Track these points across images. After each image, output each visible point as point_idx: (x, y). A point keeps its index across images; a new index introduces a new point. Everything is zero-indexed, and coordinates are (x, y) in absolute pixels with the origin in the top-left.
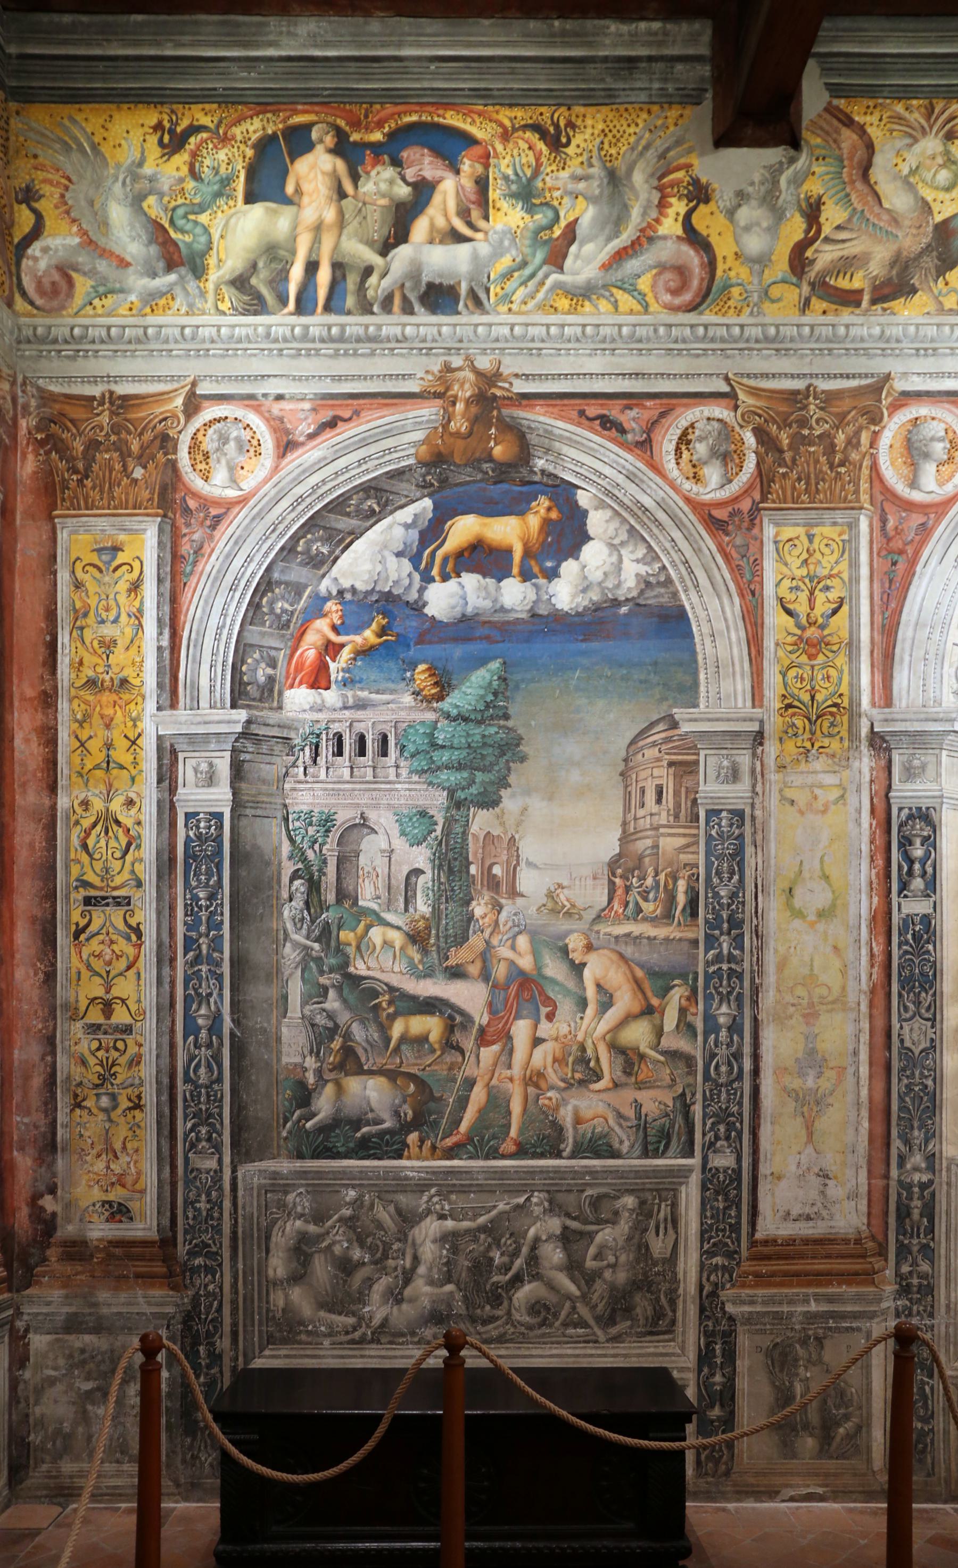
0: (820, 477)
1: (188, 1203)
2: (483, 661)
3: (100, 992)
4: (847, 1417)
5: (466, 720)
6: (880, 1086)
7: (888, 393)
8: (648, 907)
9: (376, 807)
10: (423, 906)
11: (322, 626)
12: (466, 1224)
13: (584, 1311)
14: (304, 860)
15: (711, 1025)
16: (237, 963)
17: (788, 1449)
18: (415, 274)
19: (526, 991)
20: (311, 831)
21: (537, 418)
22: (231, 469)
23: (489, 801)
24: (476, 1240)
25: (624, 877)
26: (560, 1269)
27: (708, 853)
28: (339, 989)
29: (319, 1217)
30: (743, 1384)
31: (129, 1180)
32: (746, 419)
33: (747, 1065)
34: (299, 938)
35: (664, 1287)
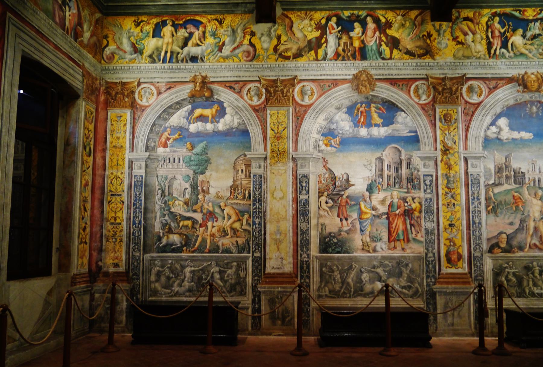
0: (280, 99)
1: (132, 263)
2: (202, 141)
3: (113, 215)
4: (288, 316)
5: (198, 155)
6: (295, 238)
8: (239, 197)
9: (178, 174)
10: (187, 196)
11: (166, 134)
12: (197, 268)
13: (224, 289)
14: (161, 186)
15: (254, 223)
16: (146, 209)
17: (274, 323)
18: (189, 54)
19: (211, 215)
20: (163, 179)
21: (215, 87)
22: (147, 99)
23: (203, 173)
24: (199, 272)
25: (234, 190)
26: (219, 279)
27: (253, 185)
28: (168, 214)
29: (162, 267)
30: (263, 308)
31: (119, 258)
32: (263, 86)
33: (263, 233)
34: (159, 203)
35: (243, 284)
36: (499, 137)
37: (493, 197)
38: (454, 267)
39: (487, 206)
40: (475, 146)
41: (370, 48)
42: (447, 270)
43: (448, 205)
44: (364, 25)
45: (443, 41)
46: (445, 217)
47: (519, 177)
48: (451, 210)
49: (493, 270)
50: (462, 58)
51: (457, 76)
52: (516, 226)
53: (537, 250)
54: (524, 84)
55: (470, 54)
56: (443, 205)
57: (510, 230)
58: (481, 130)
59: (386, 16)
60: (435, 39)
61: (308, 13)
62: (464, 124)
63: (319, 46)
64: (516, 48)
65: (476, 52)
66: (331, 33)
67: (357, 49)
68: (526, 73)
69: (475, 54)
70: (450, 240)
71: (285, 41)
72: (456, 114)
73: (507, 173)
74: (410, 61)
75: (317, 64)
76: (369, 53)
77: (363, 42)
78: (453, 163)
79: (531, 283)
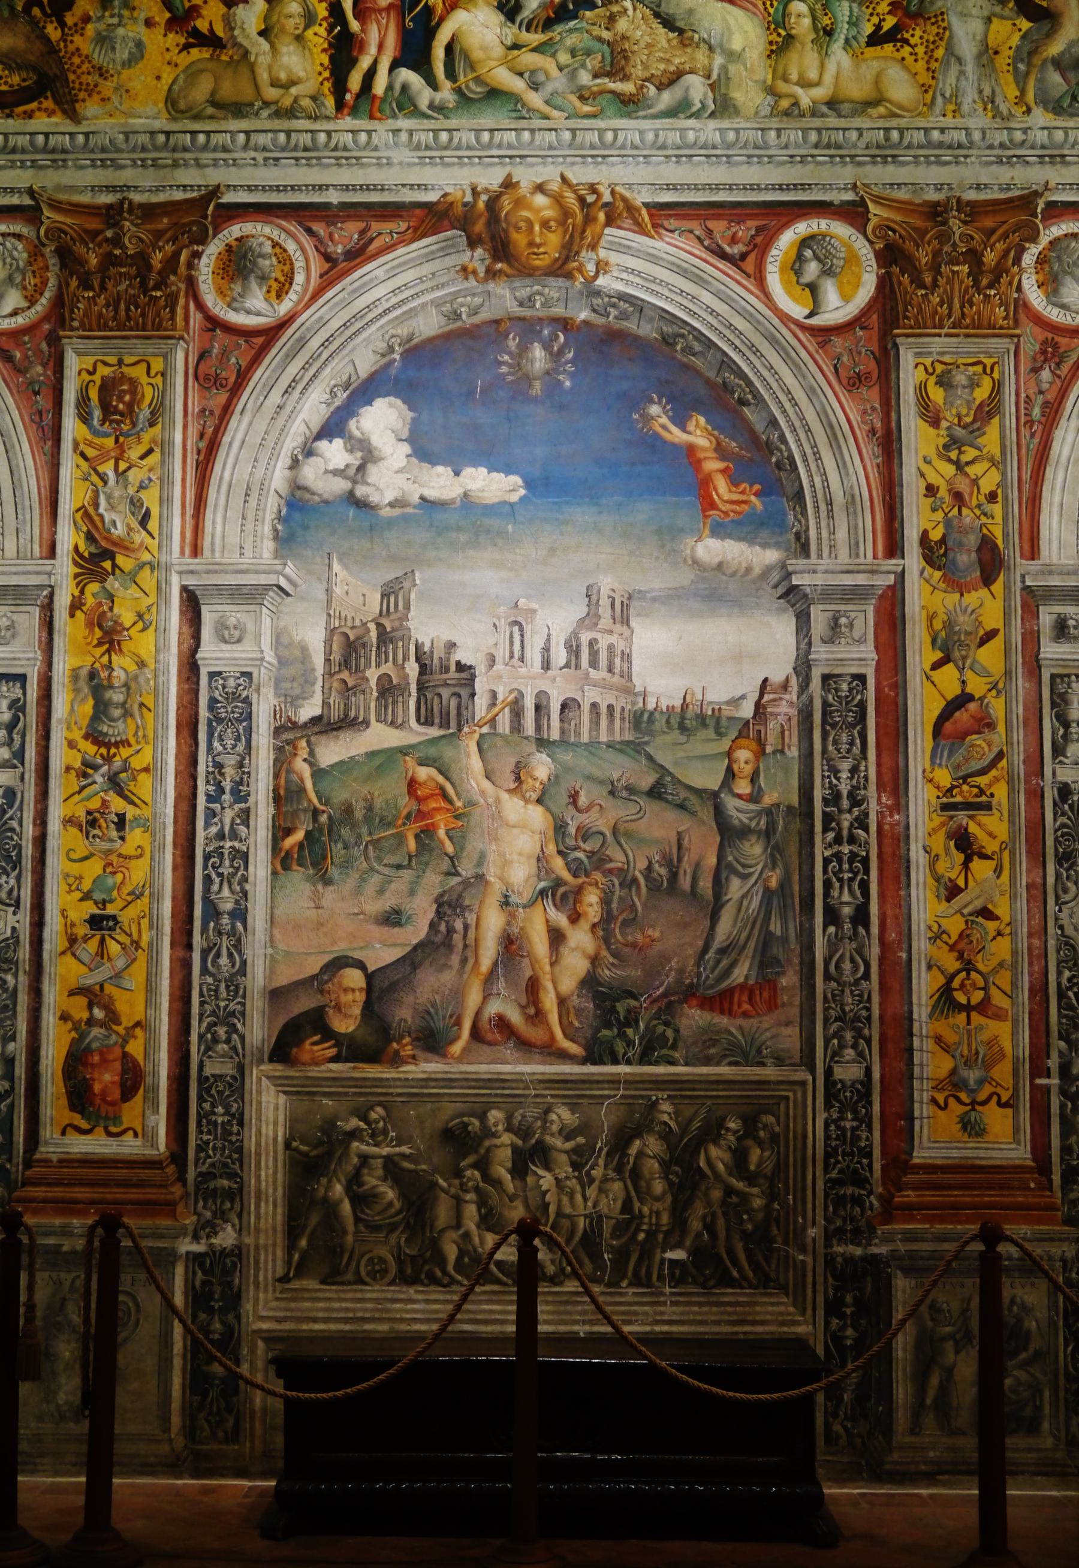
36: (360, 491)
37: (309, 784)
38: (100, 1130)
39: (280, 831)
40: (240, 537)
42: (68, 1141)
43: (93, 823)
45: (121, 31)
46: (73, 882)
47: (442, 691)
48: (105, 846)
49: (287, 1145)
50: (210, 110)
51: (179, 195)
52: (417, 931)
53: (508, 1051)
54: (493, 238)
55: (247, 93)
56: (69, 821)
57: (382, 953)
58: (274, 455)
60: (87, 19)
62: (193, 432)
64: (471, 66)
65: (275, 83)
68: (508, 184)
69: (271, 93)
70: (92, 995)
72: (159, 380)
73: (387, 668)
78: (127, 618)
79: (471, 1211)
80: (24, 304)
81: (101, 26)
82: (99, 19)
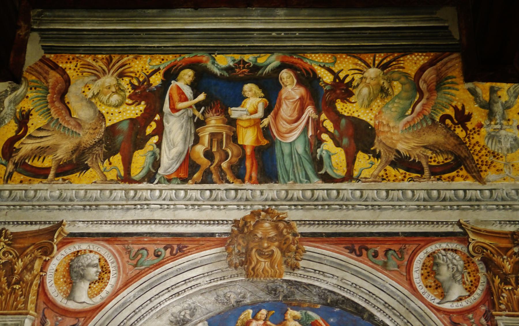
7: (60, 233)
41: (287, 150)
44: (271, 88)
45: (503, 132)
59: (336, 69)
60: (480, 126)
61: (115, 58)
63: (138, 141)
66: (174, 109)
67: (248, 151)
71: (40, 129)
74: (406, 184)
75: (127, 191)
76: (283, 164)
77: (266, 132)
80: (468, 294)
81: (490, 130)
82: (488, 126)
